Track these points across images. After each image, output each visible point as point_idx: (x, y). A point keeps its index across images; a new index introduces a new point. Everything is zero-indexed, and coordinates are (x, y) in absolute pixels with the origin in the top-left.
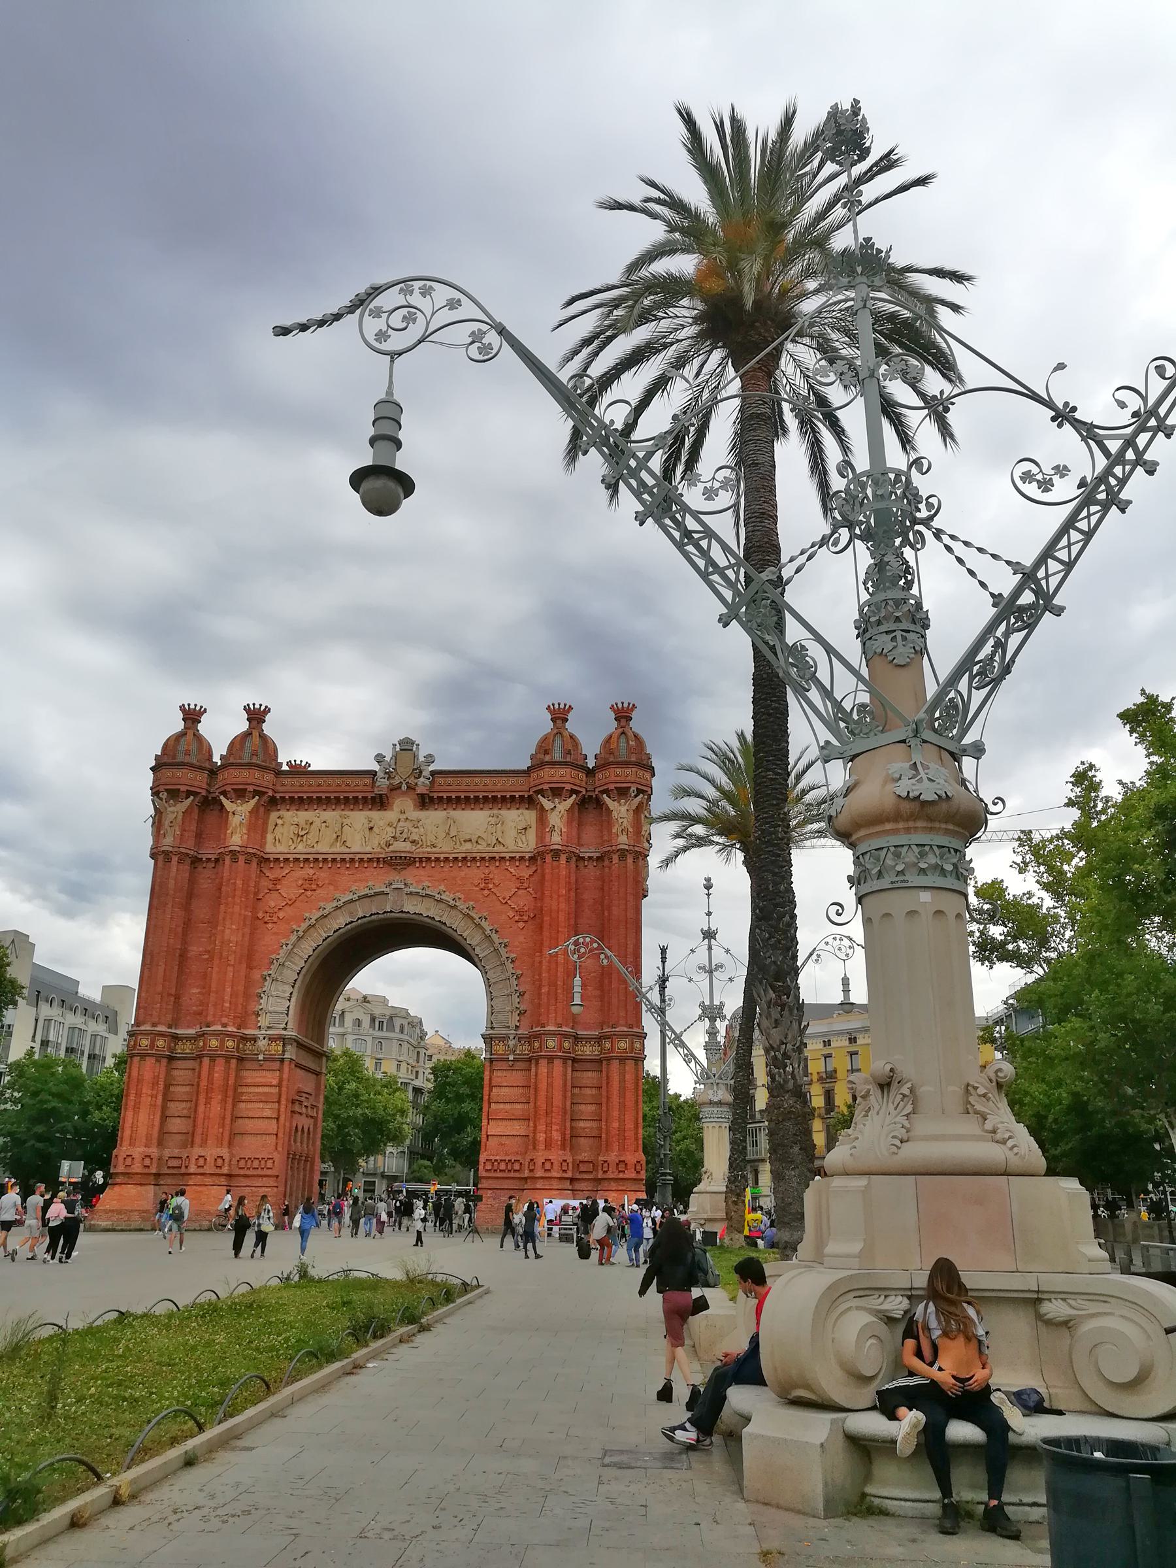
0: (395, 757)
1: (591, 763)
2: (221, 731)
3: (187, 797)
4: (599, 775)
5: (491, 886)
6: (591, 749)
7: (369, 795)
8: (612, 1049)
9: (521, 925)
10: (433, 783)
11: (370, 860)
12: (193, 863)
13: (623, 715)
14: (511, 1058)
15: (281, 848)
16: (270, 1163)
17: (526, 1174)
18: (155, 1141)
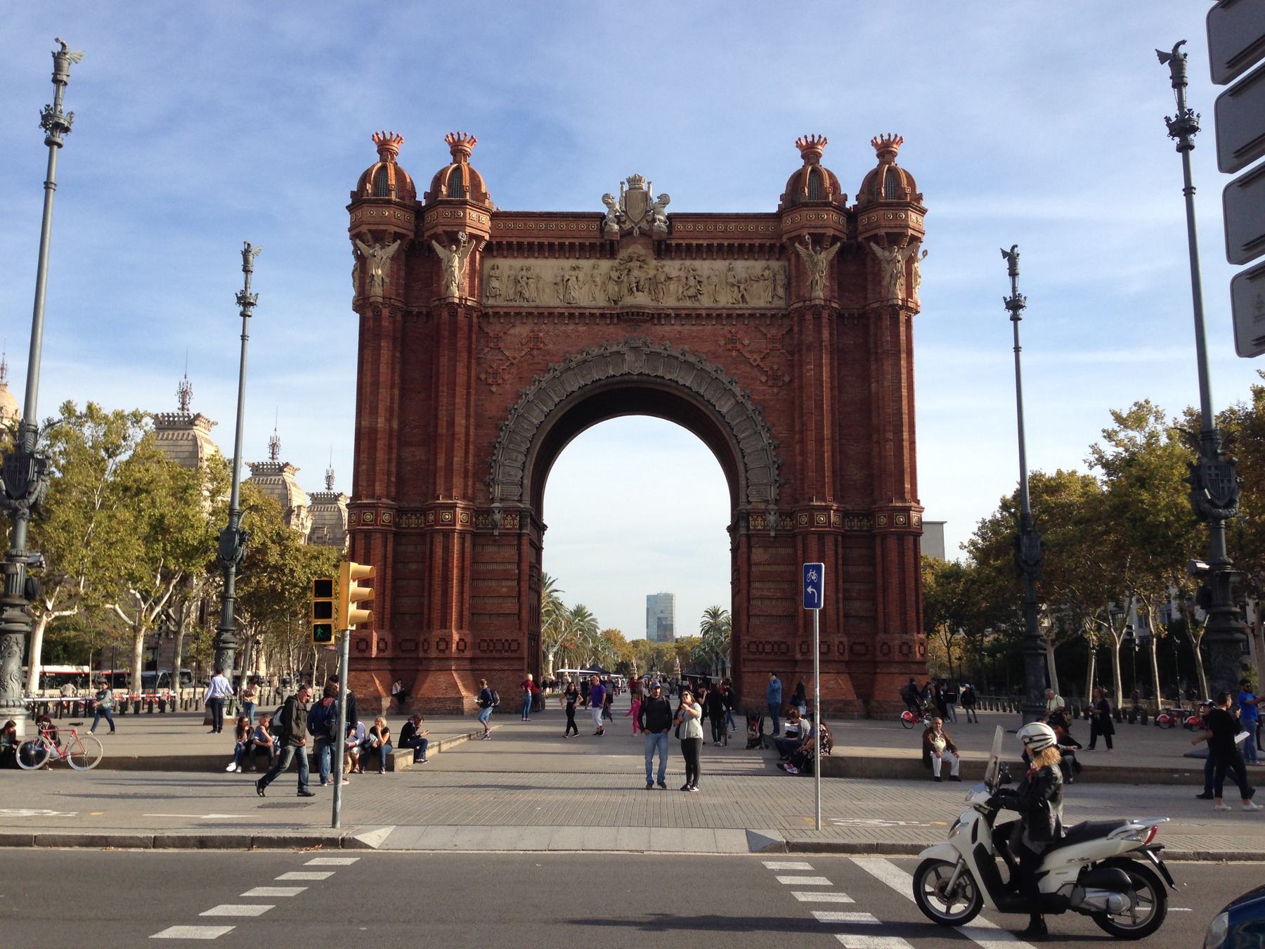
0: (626, 198)
1: (851, 203)
2: (421, 168)
3: (394, 241)
4: (863, 220)
5: (739, 346)
6: (851, 190)
7: (598, 242)
8: (891, 521)
9: (775, 390)
10: (670, 227)
11: (603, 316)
12: (403, 316)
13: (885, 150)
14: (773, 534)
15: (500, 302)
16: (514, 646)
17: (798, 656)
18: (387, 623)
